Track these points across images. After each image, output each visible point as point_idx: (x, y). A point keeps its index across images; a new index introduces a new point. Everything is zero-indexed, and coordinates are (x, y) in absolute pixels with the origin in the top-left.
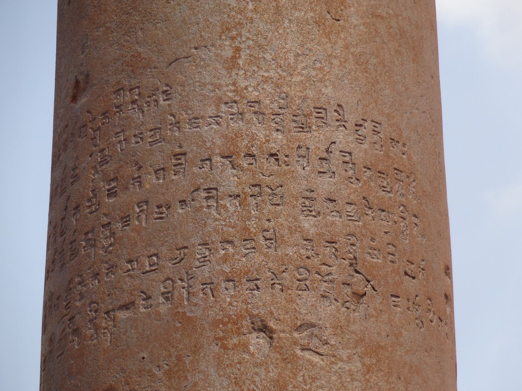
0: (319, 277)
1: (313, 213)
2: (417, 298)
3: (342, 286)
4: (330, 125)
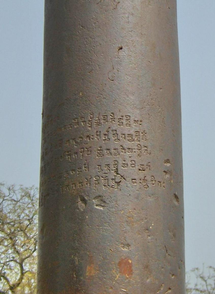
0: (103, 178)
1: (101, 155)
2: (145, 178)
3: (111, 180)
4: (108, 122)
